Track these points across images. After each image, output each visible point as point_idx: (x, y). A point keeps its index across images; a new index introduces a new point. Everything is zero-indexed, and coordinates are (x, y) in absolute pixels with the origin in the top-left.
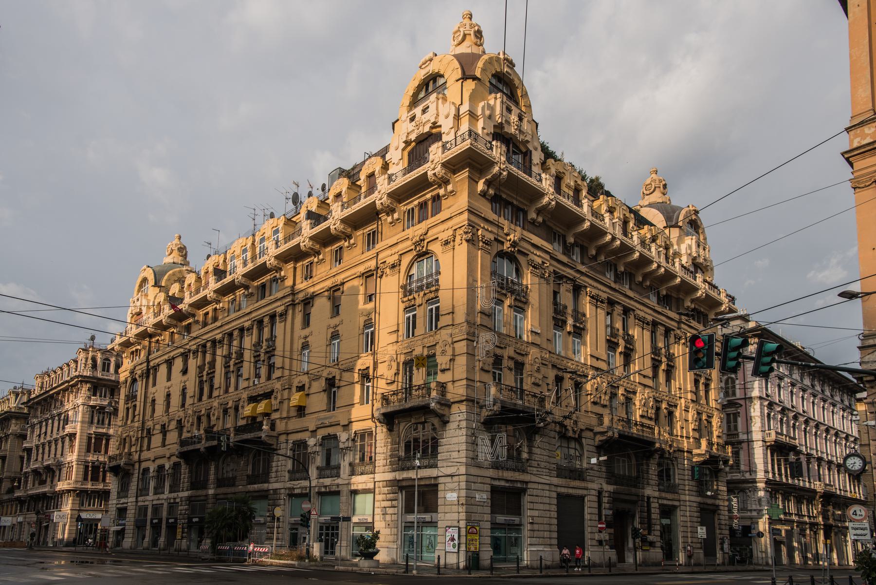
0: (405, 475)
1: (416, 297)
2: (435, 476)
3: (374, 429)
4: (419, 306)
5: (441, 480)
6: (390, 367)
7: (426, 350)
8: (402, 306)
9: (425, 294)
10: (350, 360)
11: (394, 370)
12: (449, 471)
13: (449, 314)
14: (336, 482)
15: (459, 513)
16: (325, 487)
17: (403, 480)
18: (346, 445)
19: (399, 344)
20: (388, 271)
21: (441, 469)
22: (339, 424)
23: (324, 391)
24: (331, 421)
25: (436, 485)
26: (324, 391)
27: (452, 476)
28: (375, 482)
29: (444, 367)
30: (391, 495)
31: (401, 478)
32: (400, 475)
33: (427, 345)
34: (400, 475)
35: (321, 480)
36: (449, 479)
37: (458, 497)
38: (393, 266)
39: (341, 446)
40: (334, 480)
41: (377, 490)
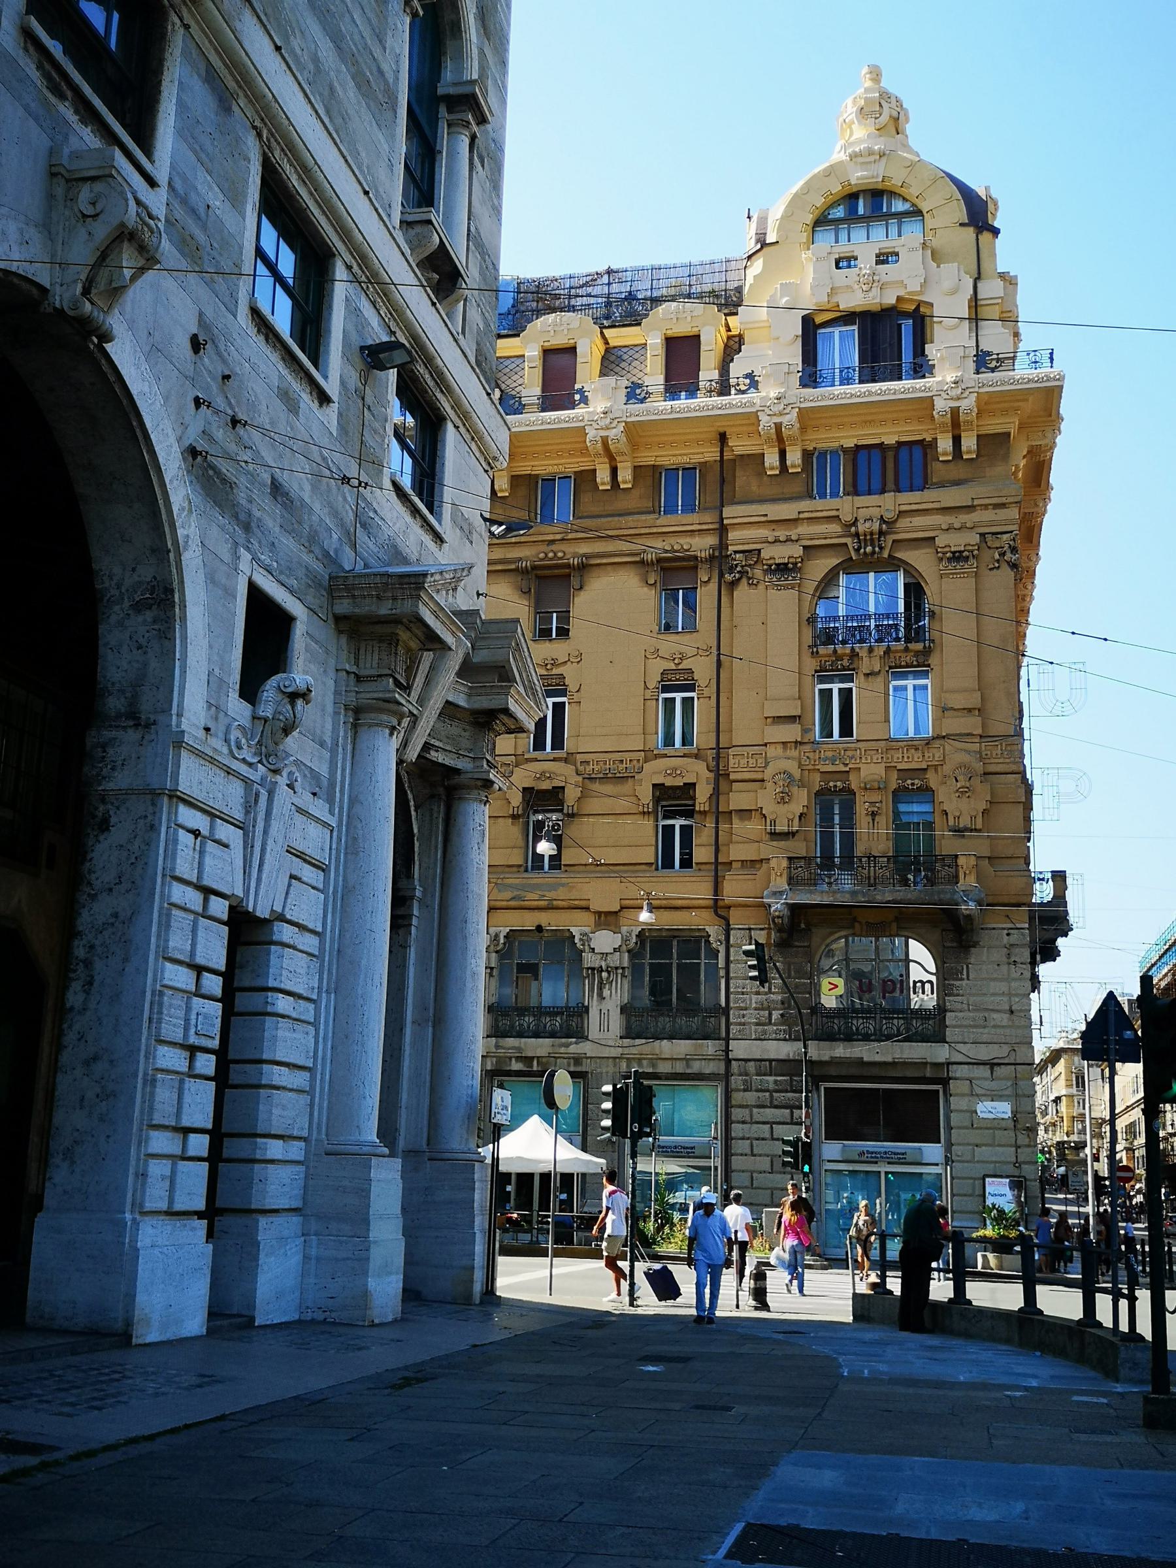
0: (840, 1050)
1: (863, 653)
2: (942, 1060)
3: (714, 931)
4: (867, 675)
5: (958, 1071)
6: (784, 798)
7: (894, 775)
8: (811, 665)
9: (888, 651)
10: (618, 756)
11: (797, 807)
12: (984, 1053)
13: (970, 710)
14: (573, 1049)
15: (1017, 1147)
16: (528, 1060)
17: (834, 1062)
18: (614, 960)
19: (807, 748)
20: (758, 573)
21: (960, 1047)
22: (587, 909)
23: (514, 817)
24: (551, 895)
25: (945, 1082)
26: (514, 817)
27: (992, 1065)
28: (728, 1062)
29: (965, 822)
30: (790, 1095)
31: (826, 1058)
32: (818, 1051)
33: (900, 766)
34: (818, 1051)
35: (511, 1042)
36: (984, 1071)
37: (1015, 1113)
38: (783, 569)
39: (589, 960)
40: (567, 1045)
41: (736, 1081)
